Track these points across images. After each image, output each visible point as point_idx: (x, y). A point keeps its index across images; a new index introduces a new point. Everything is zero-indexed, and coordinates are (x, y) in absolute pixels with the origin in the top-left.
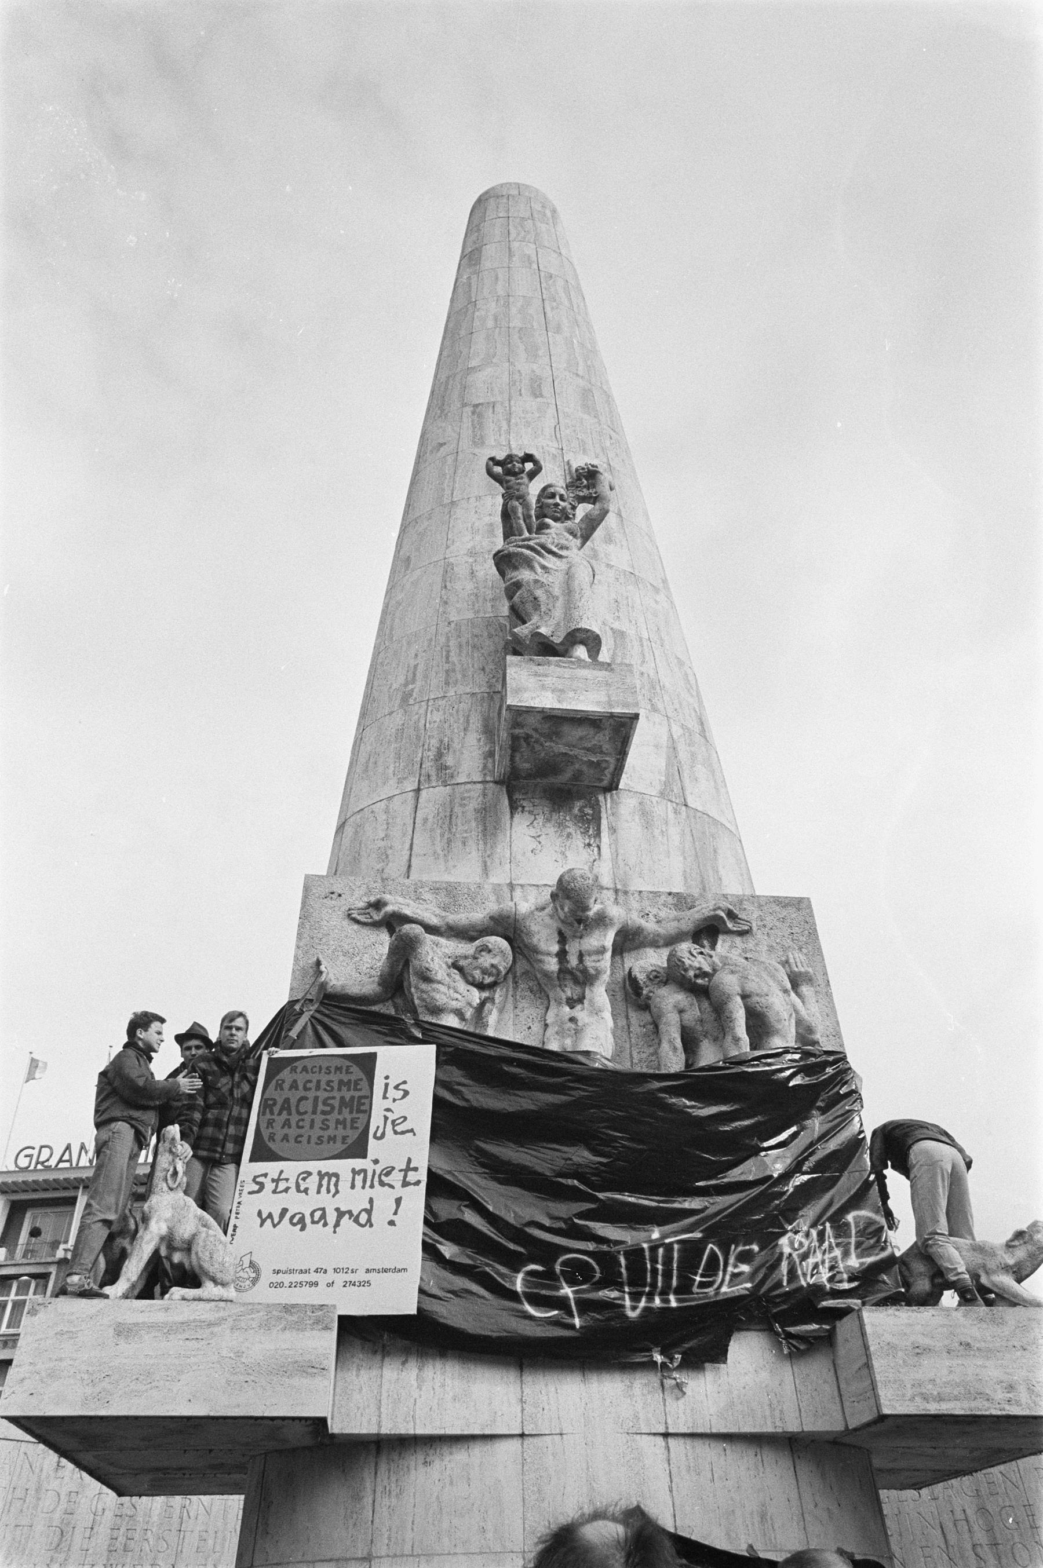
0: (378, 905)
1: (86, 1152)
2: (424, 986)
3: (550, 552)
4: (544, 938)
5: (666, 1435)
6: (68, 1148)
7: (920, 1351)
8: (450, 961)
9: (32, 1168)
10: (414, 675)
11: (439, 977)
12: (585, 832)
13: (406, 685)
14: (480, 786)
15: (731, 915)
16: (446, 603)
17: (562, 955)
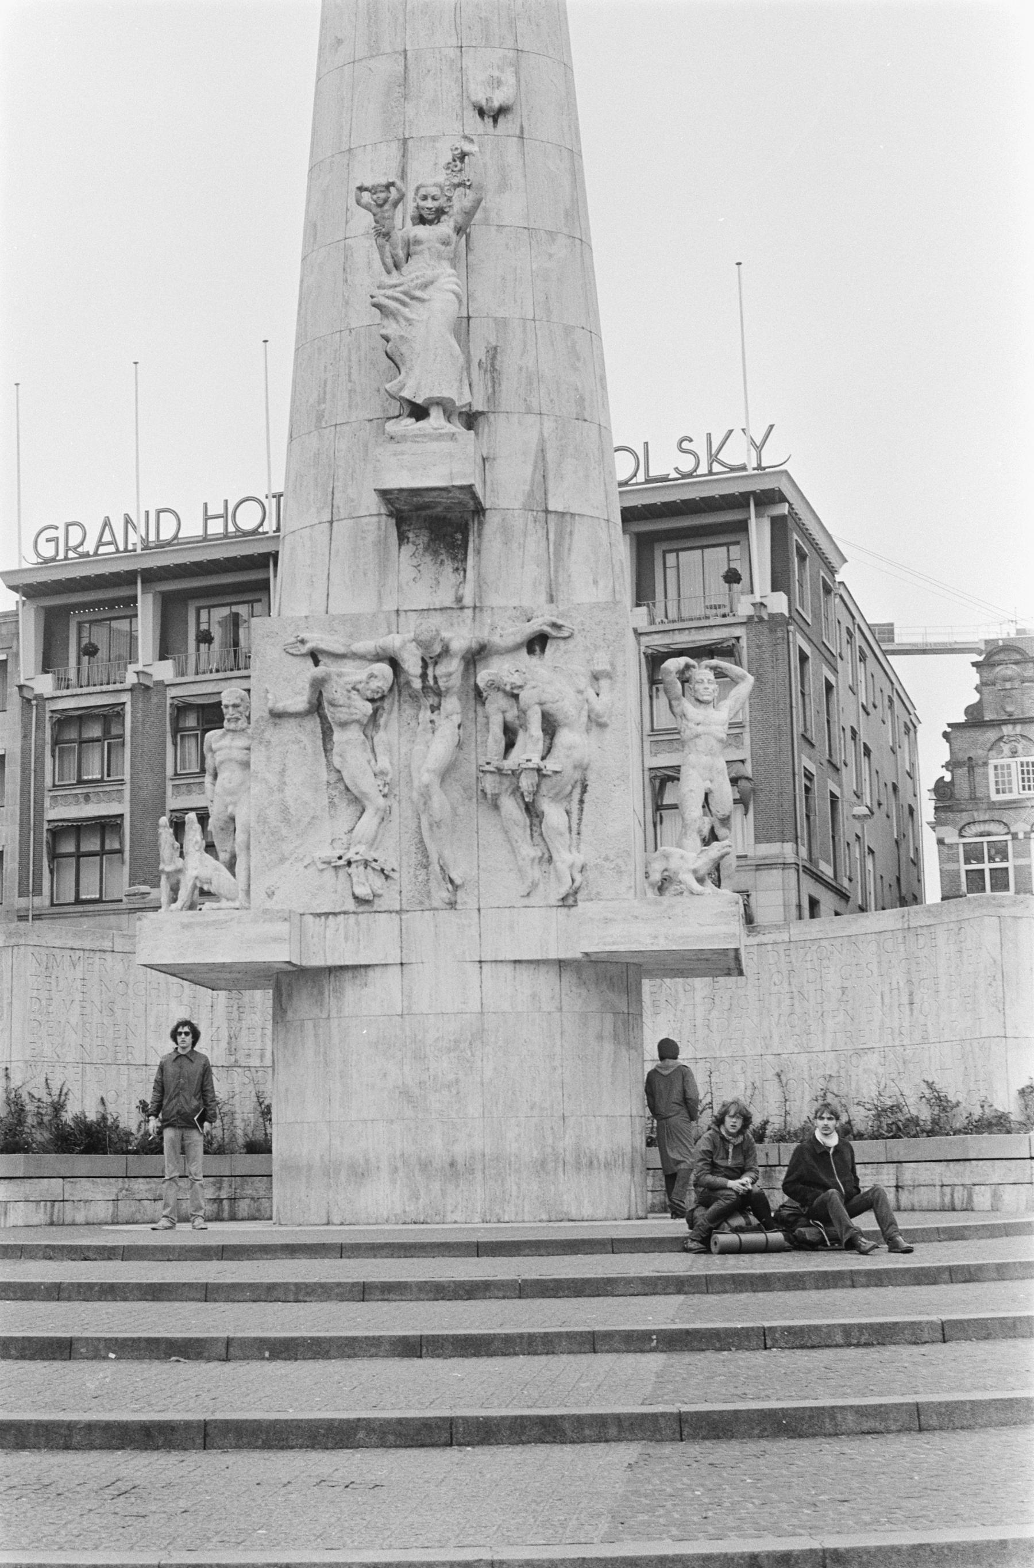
0: (303, 642)
1: (135, 528)
2: (332, 709)
3: (413, 298)
4: (412, 666)
5: (480, 962)
6: (107, 523)
7: (607, 921)
8: (349, 687)
9: (61, 556)
10: (325, 393)
11: (341, 702)
12: (454, 558)
13: (319, 403)
14: (375, 519)
15: (554, 625)
16: (347, 303)
17: (424, 676)
